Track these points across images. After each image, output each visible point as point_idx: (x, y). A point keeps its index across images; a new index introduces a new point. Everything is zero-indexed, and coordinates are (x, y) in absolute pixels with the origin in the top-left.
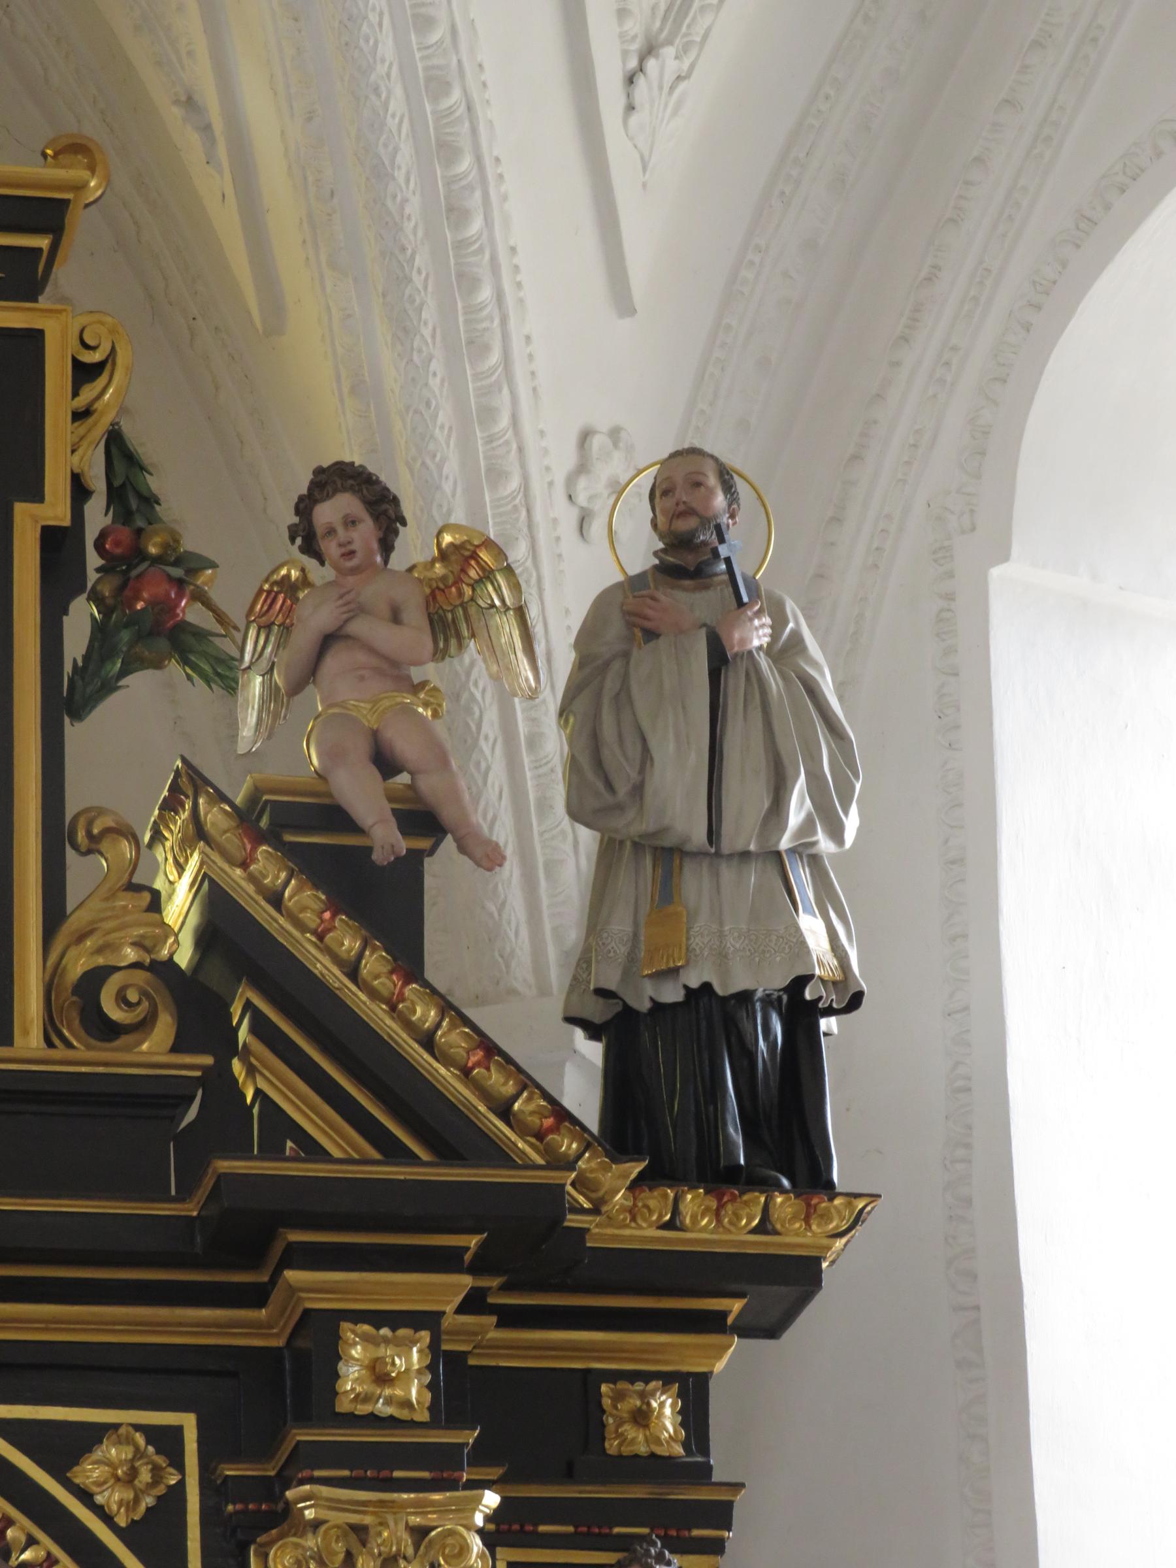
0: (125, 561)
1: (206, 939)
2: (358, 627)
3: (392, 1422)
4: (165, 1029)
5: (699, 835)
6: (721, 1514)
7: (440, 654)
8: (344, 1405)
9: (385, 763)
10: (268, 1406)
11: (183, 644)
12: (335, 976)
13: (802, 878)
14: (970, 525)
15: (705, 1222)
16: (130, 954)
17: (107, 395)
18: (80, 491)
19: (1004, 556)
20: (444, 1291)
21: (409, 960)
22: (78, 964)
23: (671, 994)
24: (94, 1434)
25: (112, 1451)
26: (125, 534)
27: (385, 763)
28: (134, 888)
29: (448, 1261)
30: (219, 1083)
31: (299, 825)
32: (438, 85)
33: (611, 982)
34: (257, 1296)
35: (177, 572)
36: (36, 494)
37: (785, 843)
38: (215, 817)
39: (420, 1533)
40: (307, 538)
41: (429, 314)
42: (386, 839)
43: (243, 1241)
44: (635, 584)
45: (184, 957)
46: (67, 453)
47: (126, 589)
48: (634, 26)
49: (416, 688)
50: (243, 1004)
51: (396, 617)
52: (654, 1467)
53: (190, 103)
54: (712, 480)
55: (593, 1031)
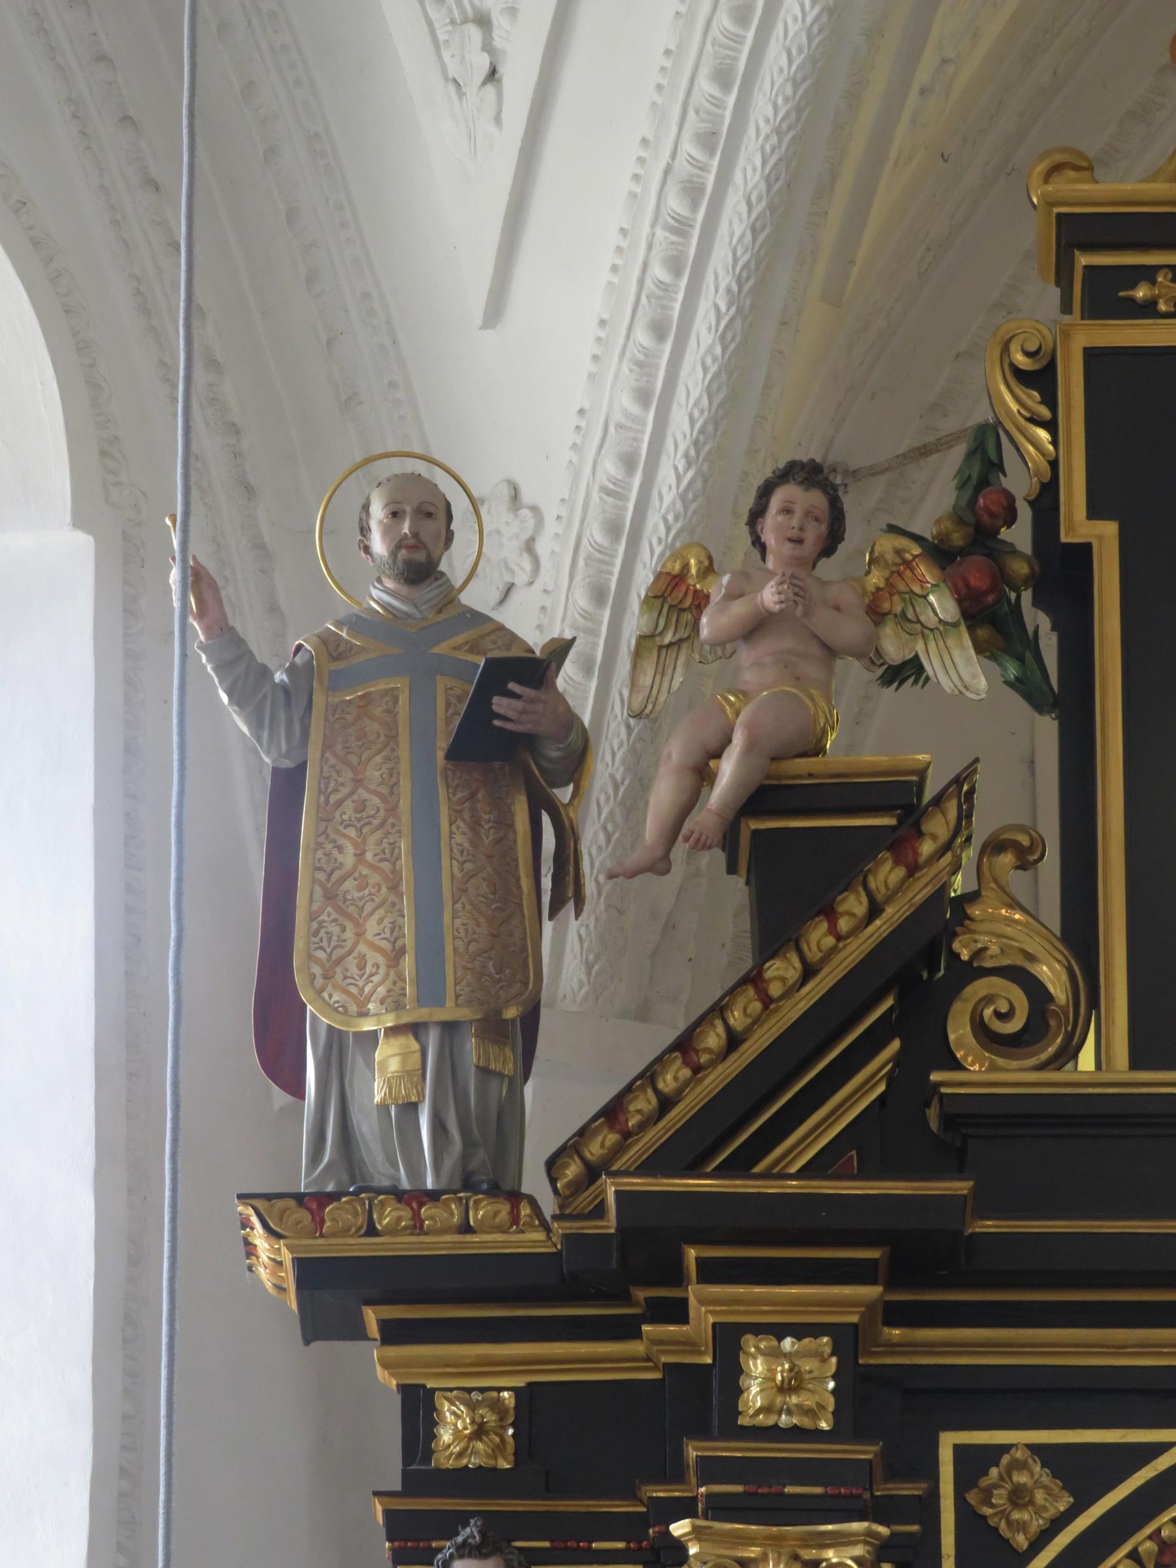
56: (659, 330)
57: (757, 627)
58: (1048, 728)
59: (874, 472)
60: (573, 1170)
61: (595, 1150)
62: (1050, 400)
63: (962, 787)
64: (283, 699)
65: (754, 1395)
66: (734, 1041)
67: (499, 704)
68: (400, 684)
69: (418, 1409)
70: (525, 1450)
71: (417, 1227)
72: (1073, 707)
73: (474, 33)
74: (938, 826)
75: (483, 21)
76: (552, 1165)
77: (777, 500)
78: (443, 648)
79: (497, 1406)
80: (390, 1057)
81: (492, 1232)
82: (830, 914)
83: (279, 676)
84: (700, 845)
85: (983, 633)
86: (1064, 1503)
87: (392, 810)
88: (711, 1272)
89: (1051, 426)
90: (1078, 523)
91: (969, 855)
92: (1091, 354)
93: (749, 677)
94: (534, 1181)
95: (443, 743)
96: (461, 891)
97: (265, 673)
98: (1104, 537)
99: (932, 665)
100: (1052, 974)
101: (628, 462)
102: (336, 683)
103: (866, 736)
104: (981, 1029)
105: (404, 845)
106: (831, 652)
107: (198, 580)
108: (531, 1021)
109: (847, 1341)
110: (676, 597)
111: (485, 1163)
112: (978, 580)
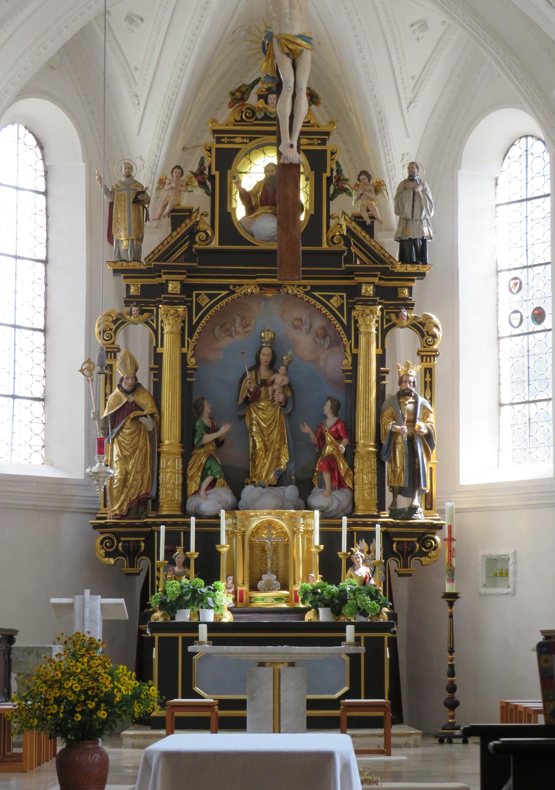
0: (338, 180)
1: (347, 232)
2: (365, 193)
3: (368, 296)
4: (342, 242)
5: (410, 217)
6: (413, 305)
7: (376, 195)
8: (362, 294)
9: (368, 211)
10: (354, 292)
11: (345, 190)
12: (363, 238)
13: (425, 222)
14: (456, 164)
15: (410, 268)
16: (338, 234)
17: (336, 157)
18: (332, 170)
19: (460, 169)
20: (376, 280)
21: (372, 236)
22: (331, 235)
23: (407, 238)
24: (333, 296)
25: (335, 298)
26: (338, 176)
27: (368, 211)
28: (338, 224)
29: (376, 276)
30: (349, 250)
31: (358, 219)
32: (380, 113)
33: (400, 236)
34: (353, 279)
35: (344, 182)
36: (326, 172)
37: (422, 218)
38: (347, 218)
39: (371, 311)
40: (359, 180)
41: (380, 142)
42: (369, 222)
43: (350, 273)
44: (405, 181)
45: (345, 234)
46: (330, 164)
47: (337, 185)
48: (409, 101)
49: (373, 200)
50: (352, 241)
51: (370, 191)
52: (405, 299)
53: (350, 109)
54: (415, 167)
55: (398, 241)
56: (160, 140)
57: (172, 188)
58: (209, 198)
59: (189, 149)
60: (148, 259)
61: (150, 257)
62: (211, 153)
63: (198, 210)
64: (110, 193)
65: (170, 289)
66: (168, 242)
67: (139, 196)
68: (126, 192)
69: (128, 287)
70: (141, 292)
71: (128, 265)
72: (212, 195)
73: (136, 98)
74: (194, 215)
75: (137, 96)
76: (145, 259)
77: (174, 171)
78: (131, 187)
79: (138, 287)
80: (125, 243)
81: (137, 265)
82: (180, 226)
83: (110, 190)
84: (164, 217)
85: (201, 186)
86: (209, 300)
87: (125, 210)
88: (165, 273)
89: (211, 157)
90: (214, 172)
91: (199, 216)
92: (216, 149)
93: (171, 195)
94: (142, 260)
95: (131, 201)
96: (134, 221)
97: (108, 190)
98: (217, 174)
99: (194, 191)
100: (209, 232)
101: (156, 156)
102: (118, 191)
103: (186, 201)
104: (200, 239)
105: (126, 215)
106: (181, 191)
107: (100, 178)
108: (142, 238)
109: (181, 282)
110: (162, 182)
111: (137, 259)
112: (201, 179)
